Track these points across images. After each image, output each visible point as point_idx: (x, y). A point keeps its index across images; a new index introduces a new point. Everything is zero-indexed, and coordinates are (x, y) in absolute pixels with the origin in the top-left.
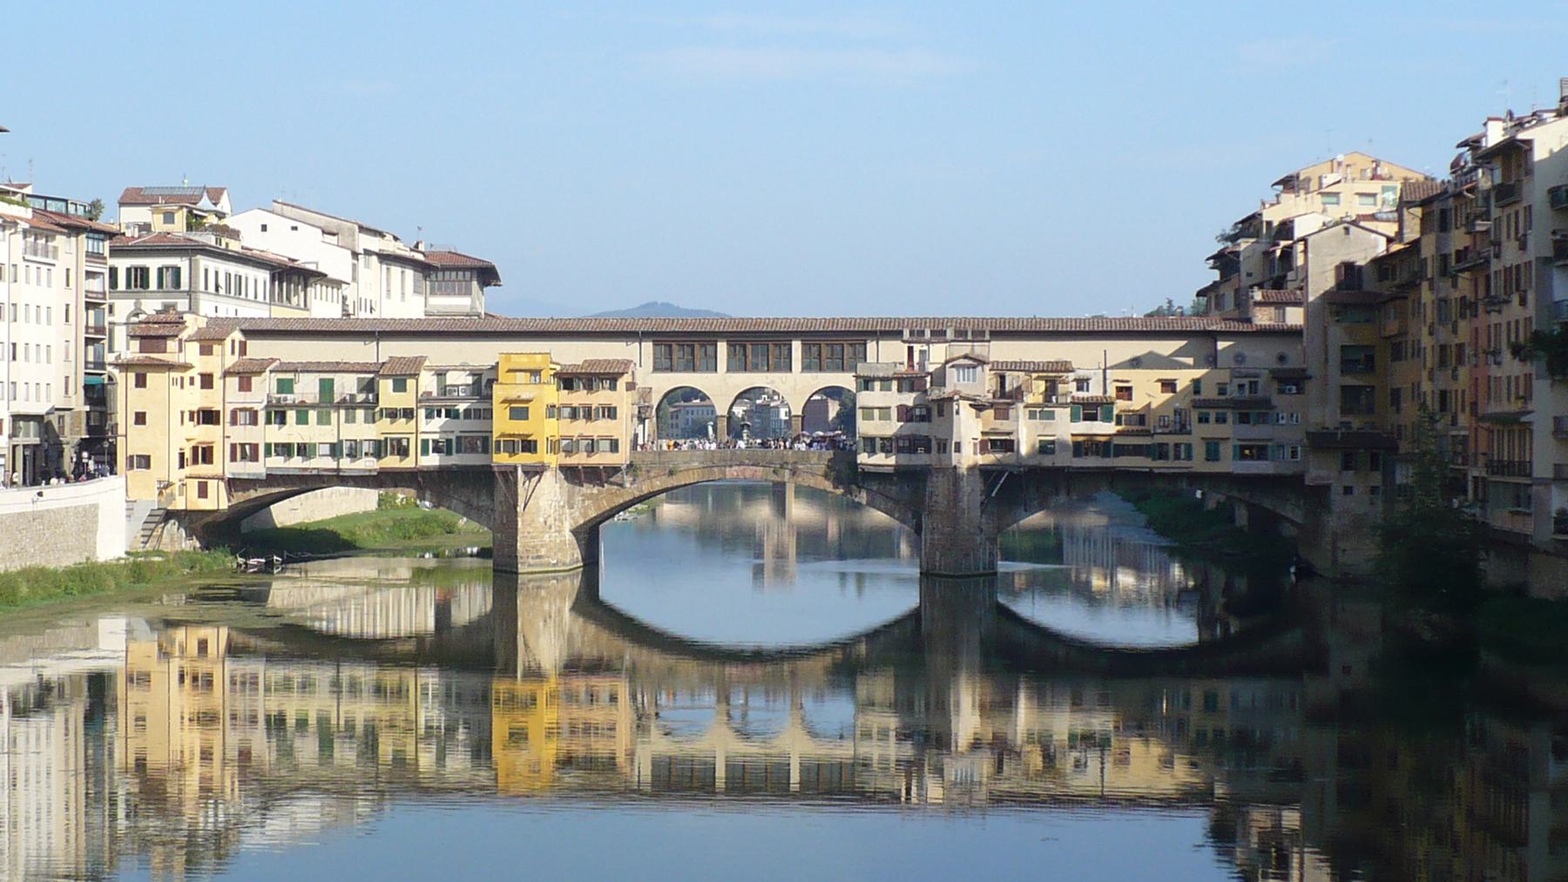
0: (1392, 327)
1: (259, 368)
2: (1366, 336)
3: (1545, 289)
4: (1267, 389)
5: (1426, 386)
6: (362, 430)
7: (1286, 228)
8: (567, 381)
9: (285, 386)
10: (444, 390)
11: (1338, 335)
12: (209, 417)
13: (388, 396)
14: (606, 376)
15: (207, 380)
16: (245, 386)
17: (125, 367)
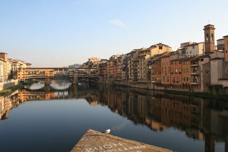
0: (104, 68)
1: (27, 71)
2: (101, 69)
3: (123, 66)
4: (95, 72)
5: (108, 71)
6: (35, 75)
7: (91, 62)
8: (50, 72)
9: (29, 72)
10: (41, 73)
11: (100, 68)
12: (24, 75)
13: (37, 73)
14: (52, 71)
15: (23, 72)
16: (26, 72)
17: (18, 71)
